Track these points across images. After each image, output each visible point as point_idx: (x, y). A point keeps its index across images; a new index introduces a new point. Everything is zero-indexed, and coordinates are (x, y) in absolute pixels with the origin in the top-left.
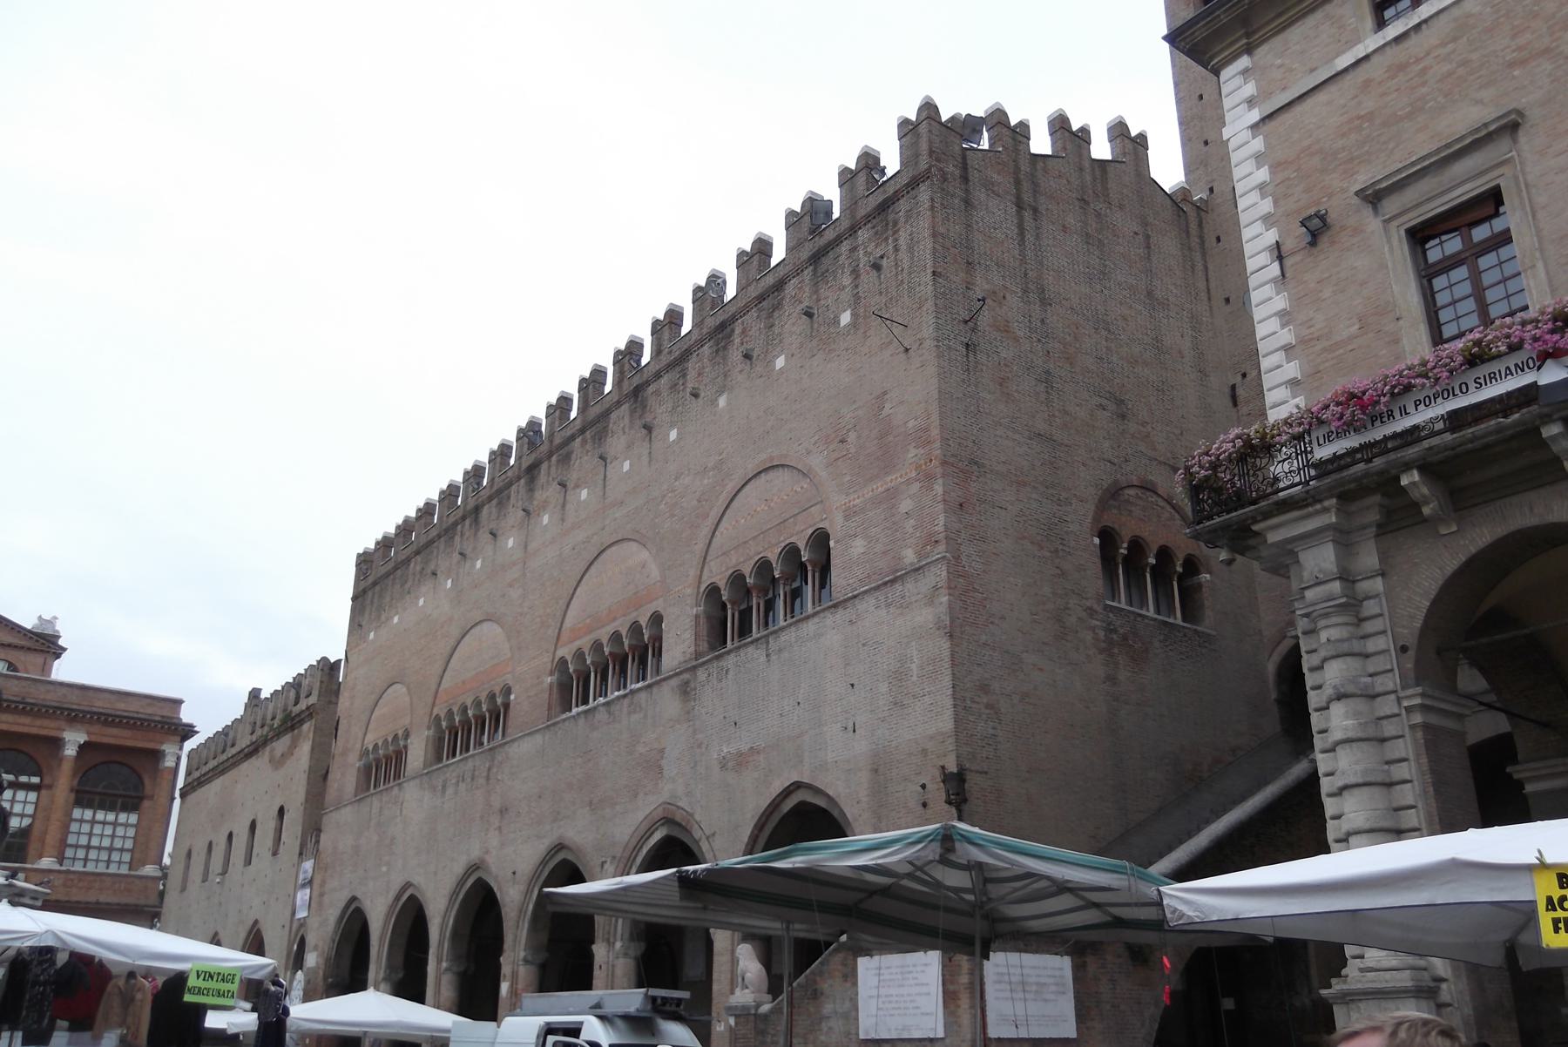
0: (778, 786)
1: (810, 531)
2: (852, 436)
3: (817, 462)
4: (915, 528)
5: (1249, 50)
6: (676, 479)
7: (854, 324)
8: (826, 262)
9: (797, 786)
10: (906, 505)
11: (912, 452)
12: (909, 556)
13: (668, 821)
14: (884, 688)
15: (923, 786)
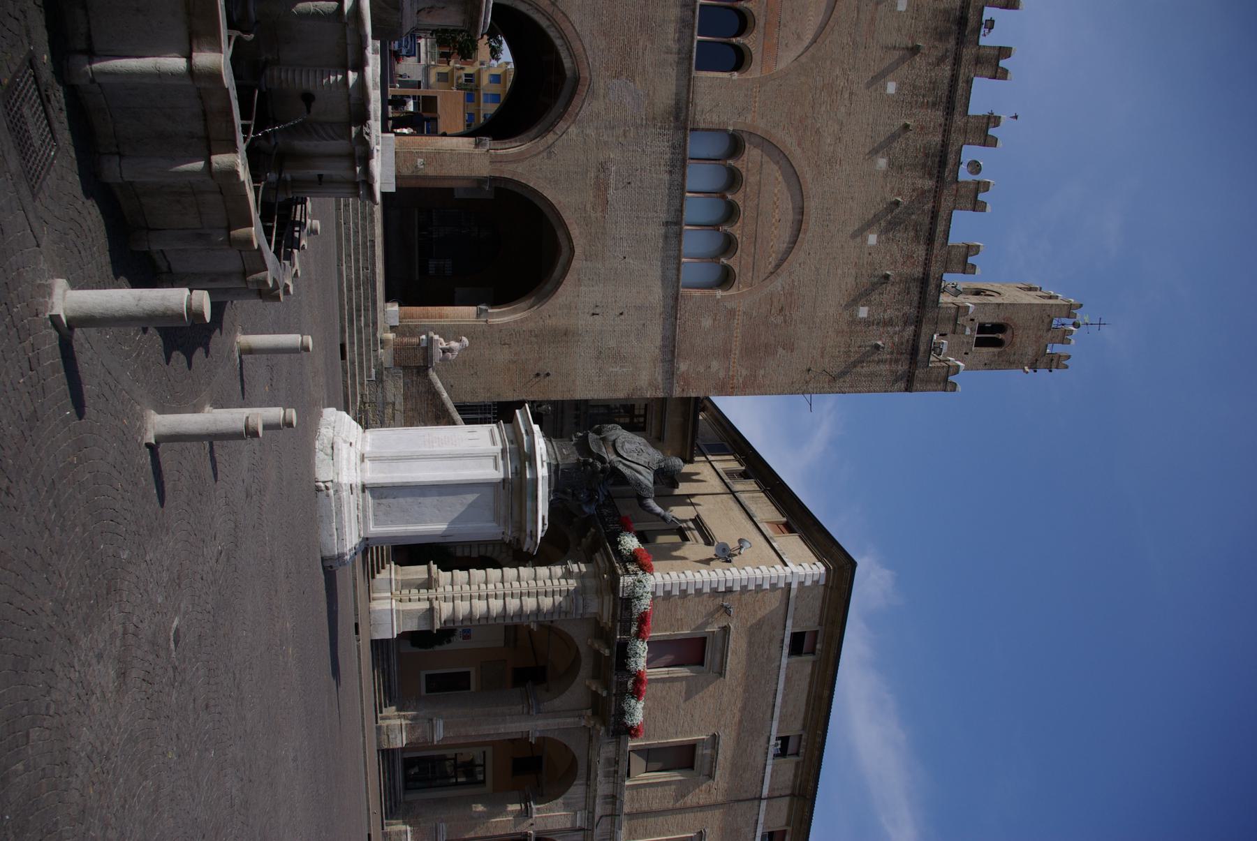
0: (575, 231)
1: (737, 271)
2: (780, 319)
3: (778, 284)
4: (698, 373)
5: (826, 586)
6: (851, 94)
7: (854, 321)
8: (915, 291)
9: (572, 250)
10: (715, 365)
11: (744, 372)
12: (683, 367)
13: (577, 80)
14: (612, 343)
15: (548, 374)
